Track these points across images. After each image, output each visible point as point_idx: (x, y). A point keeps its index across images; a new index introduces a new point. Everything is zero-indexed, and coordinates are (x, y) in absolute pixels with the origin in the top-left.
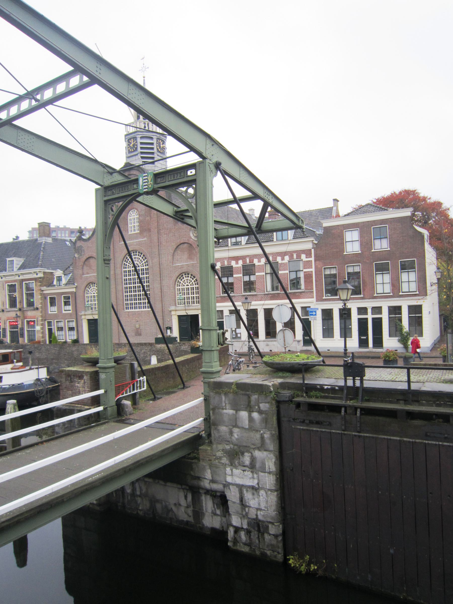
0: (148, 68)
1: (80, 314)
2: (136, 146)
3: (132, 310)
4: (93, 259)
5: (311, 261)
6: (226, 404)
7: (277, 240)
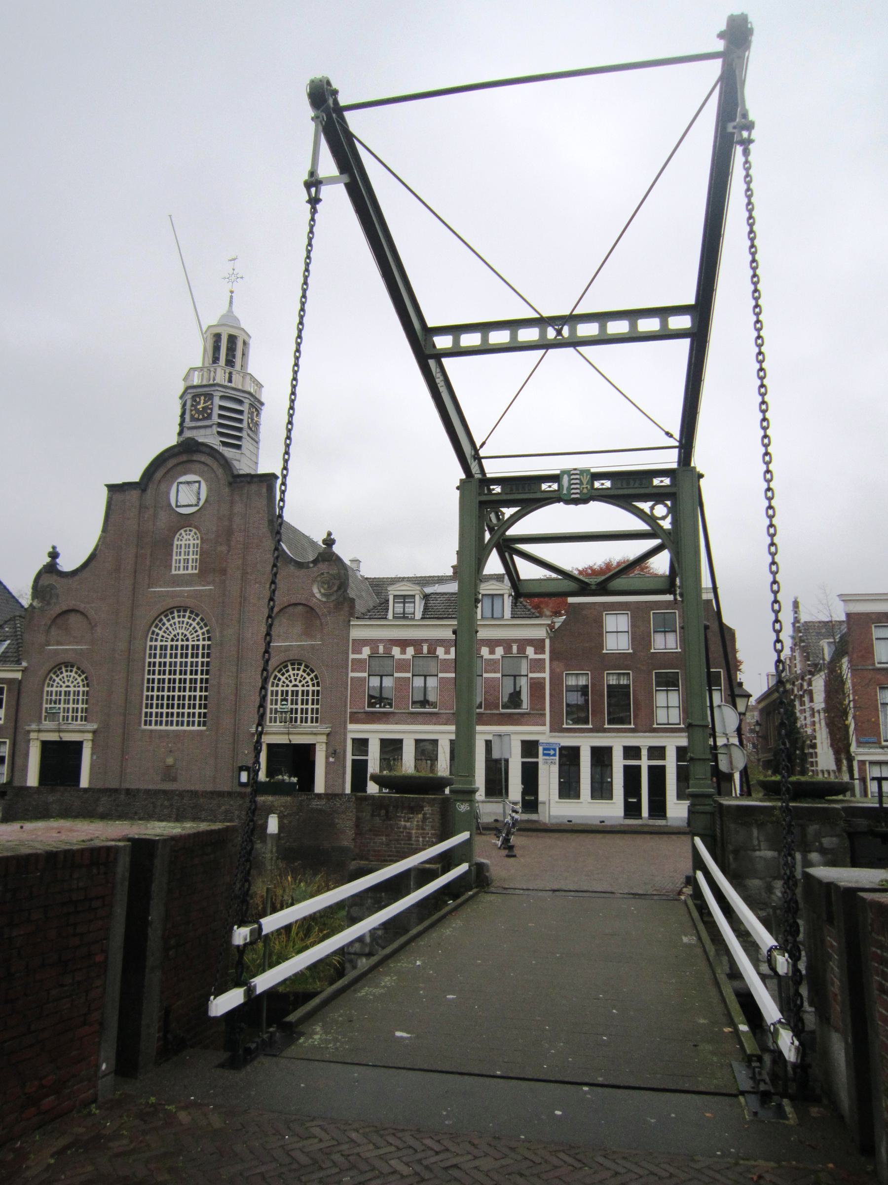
0: (242, 278)
1: (27, 728)
2: (209, 411)
3: (159, 728)
4: (79, 617)
5: (544, 659)
6: (759, 841)
7: (482, 617)
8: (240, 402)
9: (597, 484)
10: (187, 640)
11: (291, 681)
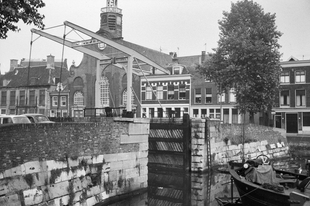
5: (190, 85)
10: (104, 83)
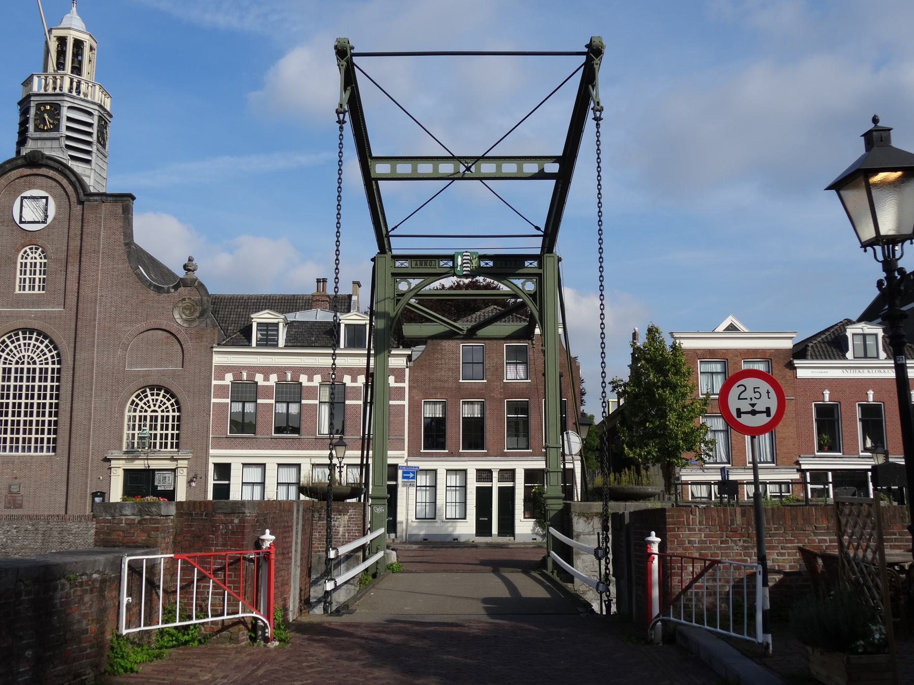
8: (90, 114)
9: (482, 264)
10: (35, 363)
11: (149, 407)
